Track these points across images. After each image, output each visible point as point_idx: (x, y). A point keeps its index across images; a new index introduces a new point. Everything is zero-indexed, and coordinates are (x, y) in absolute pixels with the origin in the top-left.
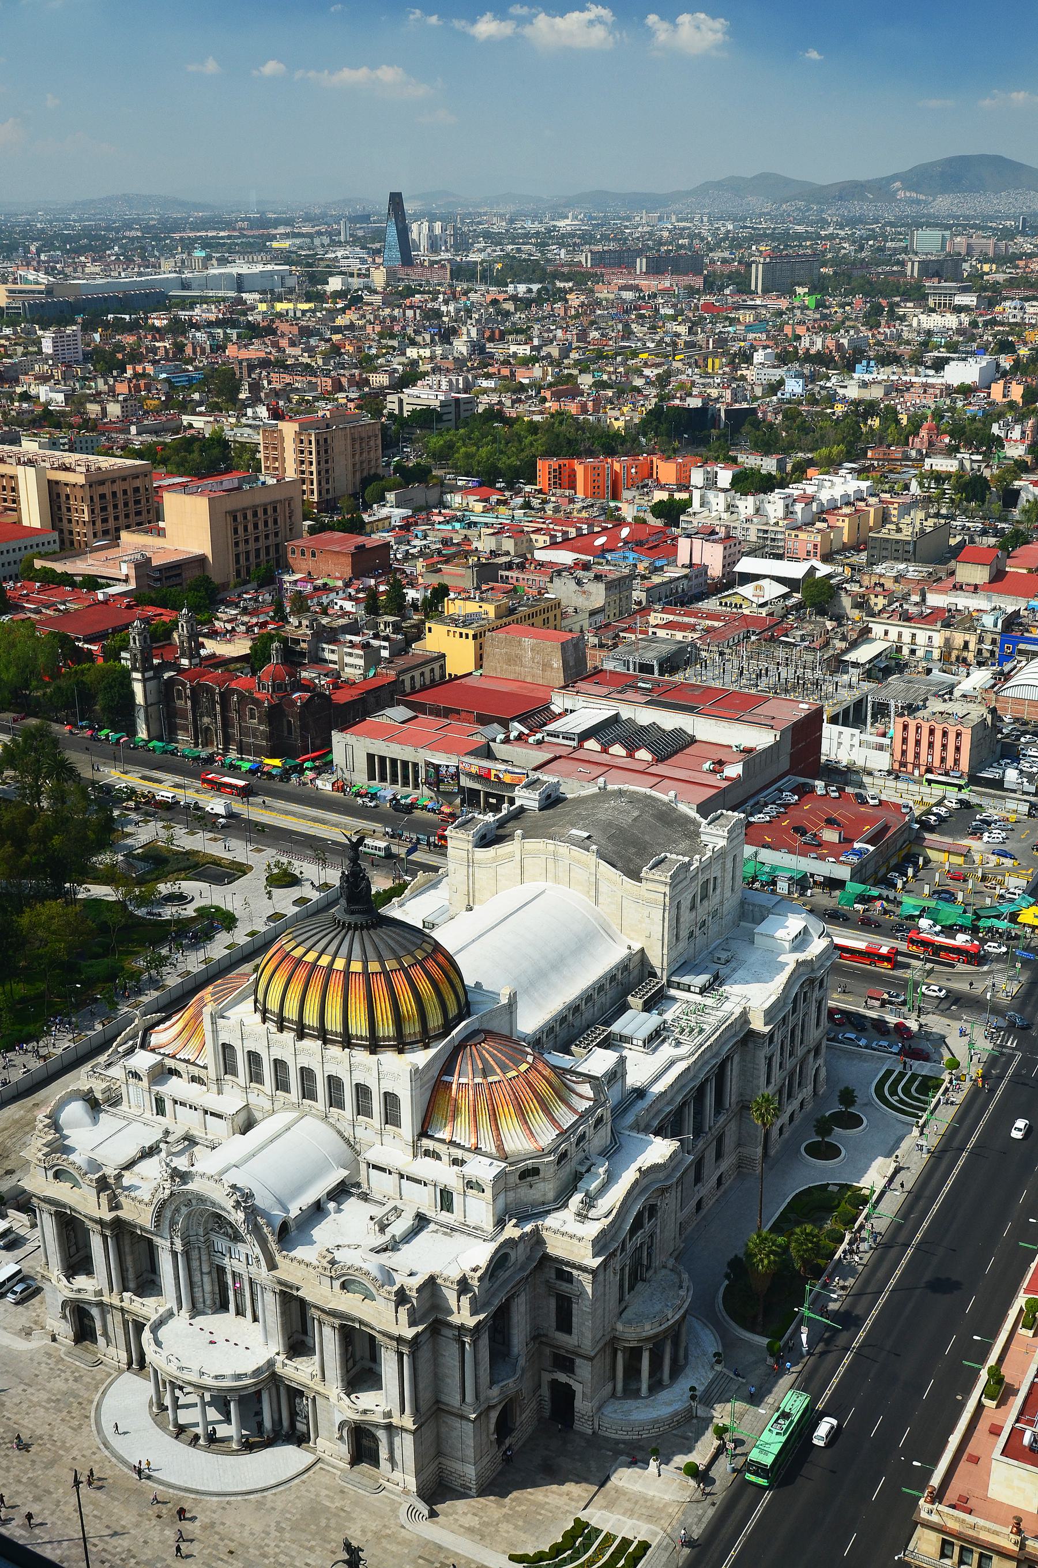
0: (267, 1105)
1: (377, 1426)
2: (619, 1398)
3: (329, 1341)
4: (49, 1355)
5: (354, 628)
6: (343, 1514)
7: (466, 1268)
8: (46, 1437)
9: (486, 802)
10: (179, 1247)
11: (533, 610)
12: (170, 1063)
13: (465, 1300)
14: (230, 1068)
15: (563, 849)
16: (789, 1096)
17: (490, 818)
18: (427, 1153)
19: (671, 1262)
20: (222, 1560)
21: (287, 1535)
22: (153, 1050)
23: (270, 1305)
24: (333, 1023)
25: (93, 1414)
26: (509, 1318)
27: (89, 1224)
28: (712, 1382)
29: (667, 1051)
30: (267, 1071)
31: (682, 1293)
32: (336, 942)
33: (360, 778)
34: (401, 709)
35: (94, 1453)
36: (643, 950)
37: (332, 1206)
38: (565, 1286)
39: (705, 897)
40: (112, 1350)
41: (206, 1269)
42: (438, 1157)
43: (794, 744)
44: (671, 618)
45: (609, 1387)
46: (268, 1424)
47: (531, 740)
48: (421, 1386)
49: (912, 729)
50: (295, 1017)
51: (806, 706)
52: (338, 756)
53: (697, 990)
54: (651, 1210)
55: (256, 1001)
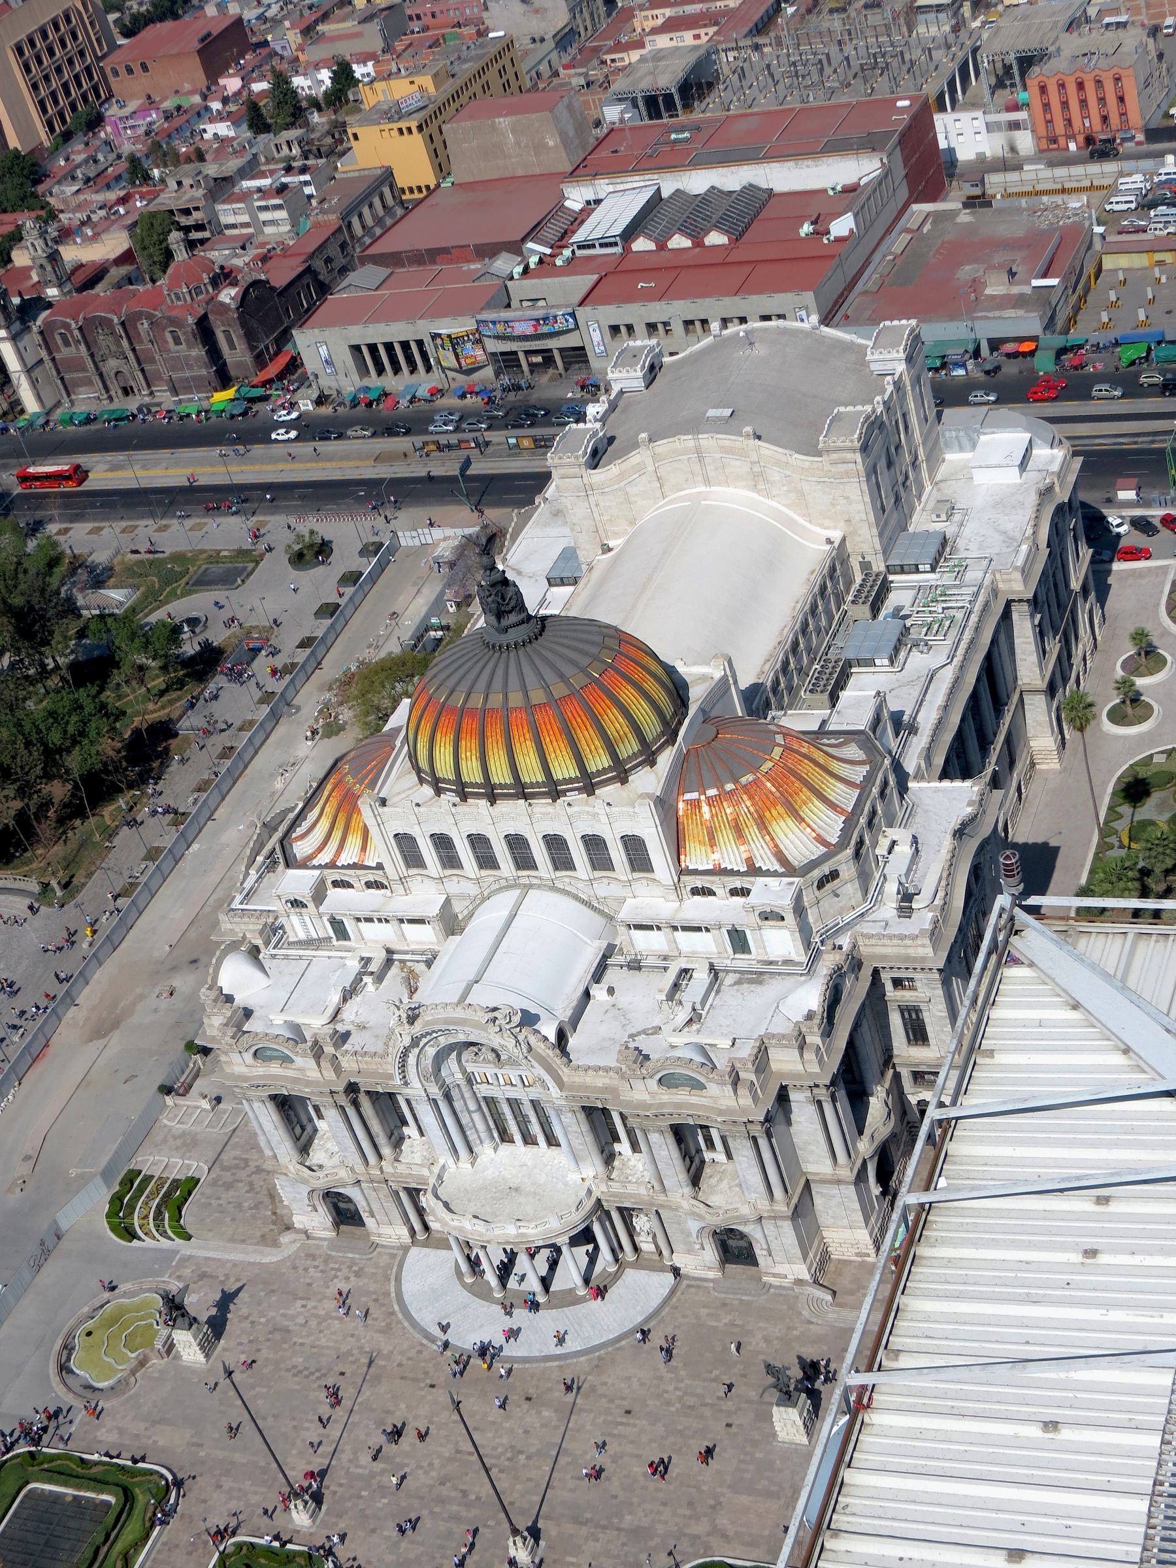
0: (473, 890)
4: (313, 1257)
5: (251, 169)
6: (736, 1330)
7: (799, 1017)
8: (355, 1352)
9: (530, 365)
10: (435, 1091)
11: (482, 63)
12: (335, 875)
13: (810, 1056)
14: (413, 859)
15: (706, 440)
18: (695, 891)
20: (622, 1424)
21: (683, 1373)
22: (303, 865)
23: (571, 1127)
24: (531, 772)
25: (396, 1307)
26: (856, 1054)
27: (317, 1100)
29: (917, 662)
30: (464, 851)
32: (500, 672)
34: (370, 268)
35: (419, 1352)
36: (844, 540)
40: (386, 1230)
41: (472, 1106)
42: (711, 893)
43: (906, 162)
44: (668, 12)
47: (559, 262)
49: (1052, 89)
50: (478, 778)
51: (906, 103)
52: (311, 364)
53: (928, 568)
55: (419, 771)
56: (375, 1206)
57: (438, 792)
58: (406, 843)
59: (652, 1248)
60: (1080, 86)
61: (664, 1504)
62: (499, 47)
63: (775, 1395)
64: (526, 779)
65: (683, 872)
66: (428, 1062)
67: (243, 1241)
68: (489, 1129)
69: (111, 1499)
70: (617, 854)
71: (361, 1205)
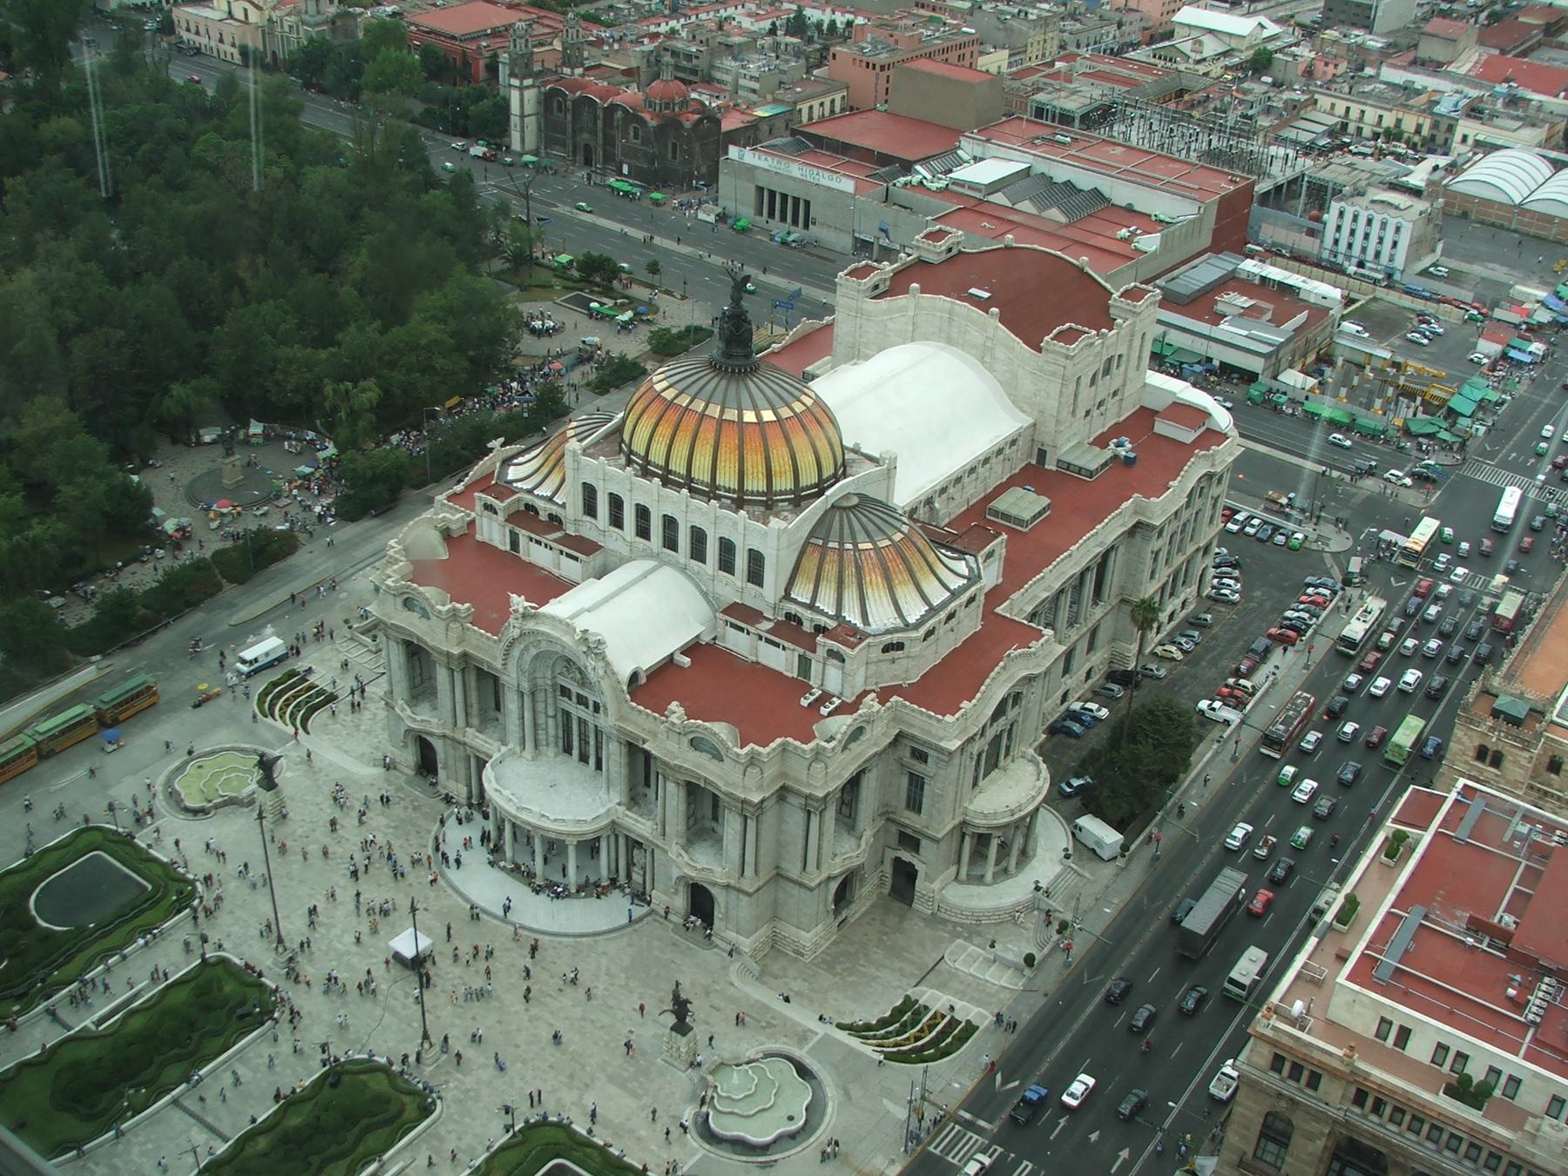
1: (715, 884)
2: (961, 883)
3: (673, 799)
10: (525, 686)
11: (949, 44)
14: (590, 510)
15: (964, 307)
16: (1171, 595)
17: (888, 267)
19: (1031, 751)
23: (614, 755)
24: (701, 472)
28: (1058, 877)
31: (1039, 783)
33: (746, 213)
36: (1034, 425)
37: (686, 661)
38: (918, 767)
39: (1107, 372)
41: (551, 713)
43: (1219, 218)
45: (953, 869)
46: (604, 872)
48: (762, 851)
49: (1348, 217)
54: (1016, 698)
56: (451, 762)
57: (629, 462)
58: (589, 492)
59: (640, 880)
60: (1369, 222)
61: (551, 1067)
62: (966, 39)
63: (671, 1020)
64: (695, 475)
65: (787, 596)
66: (528, 658)
67: (346, 752)
68: (556, 737)
69: (150, 887)
70: (741, 562)
71: (440, 756)
